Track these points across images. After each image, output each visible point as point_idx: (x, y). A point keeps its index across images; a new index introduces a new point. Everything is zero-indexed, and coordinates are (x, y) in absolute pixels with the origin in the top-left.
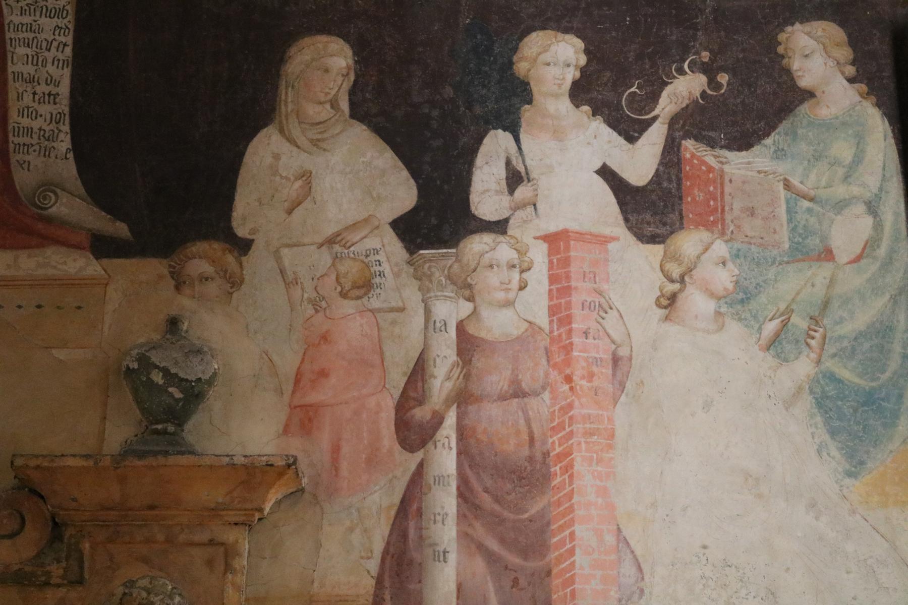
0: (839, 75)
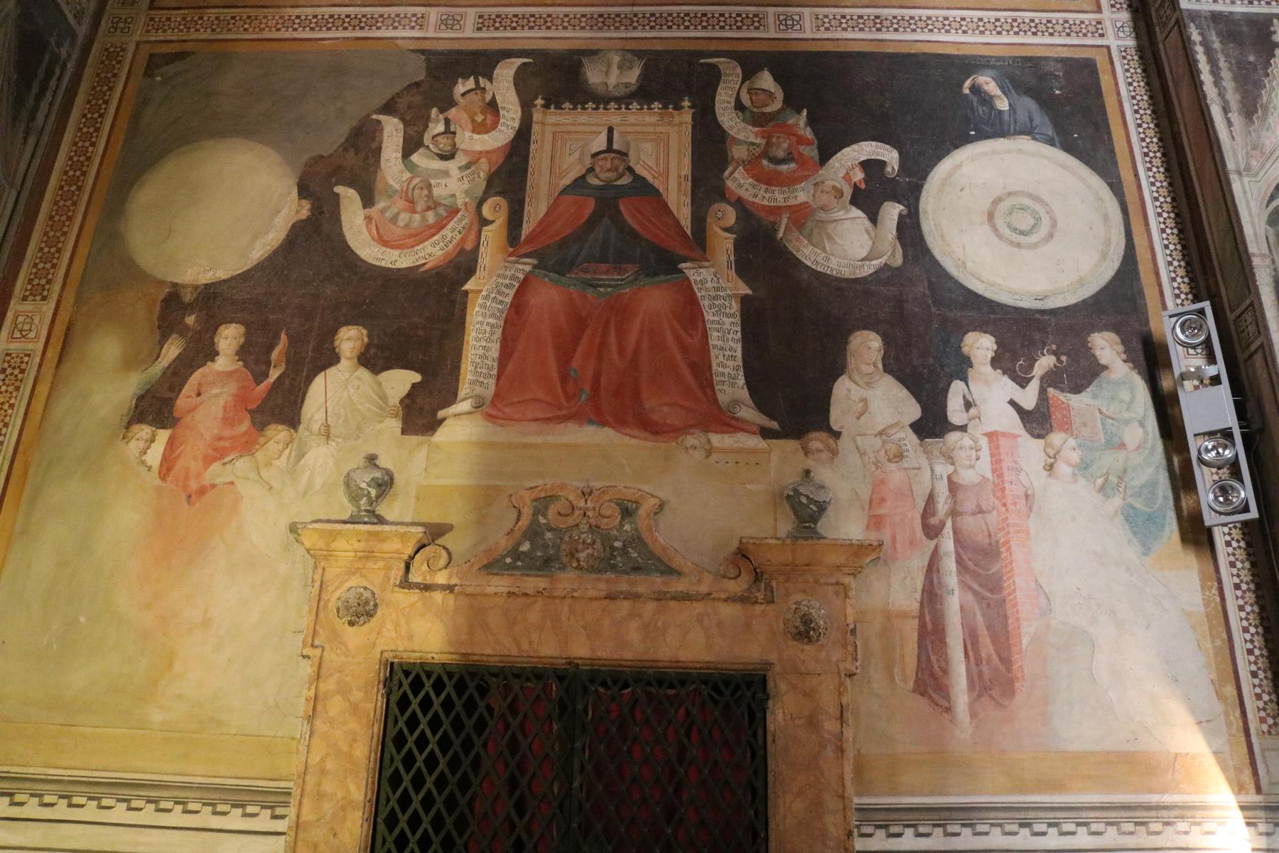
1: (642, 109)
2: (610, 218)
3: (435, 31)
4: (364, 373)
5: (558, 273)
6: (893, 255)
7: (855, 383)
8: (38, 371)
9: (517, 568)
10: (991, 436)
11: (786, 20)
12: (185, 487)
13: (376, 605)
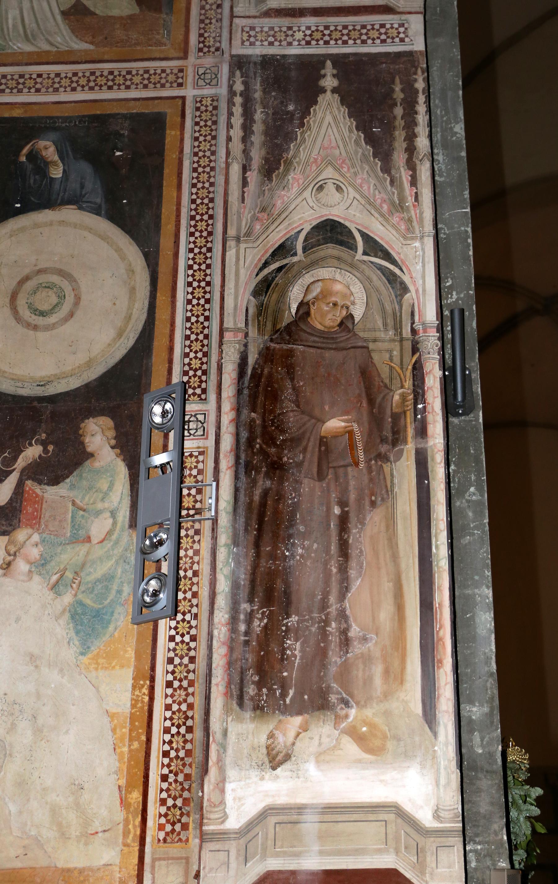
0: (107, 445)
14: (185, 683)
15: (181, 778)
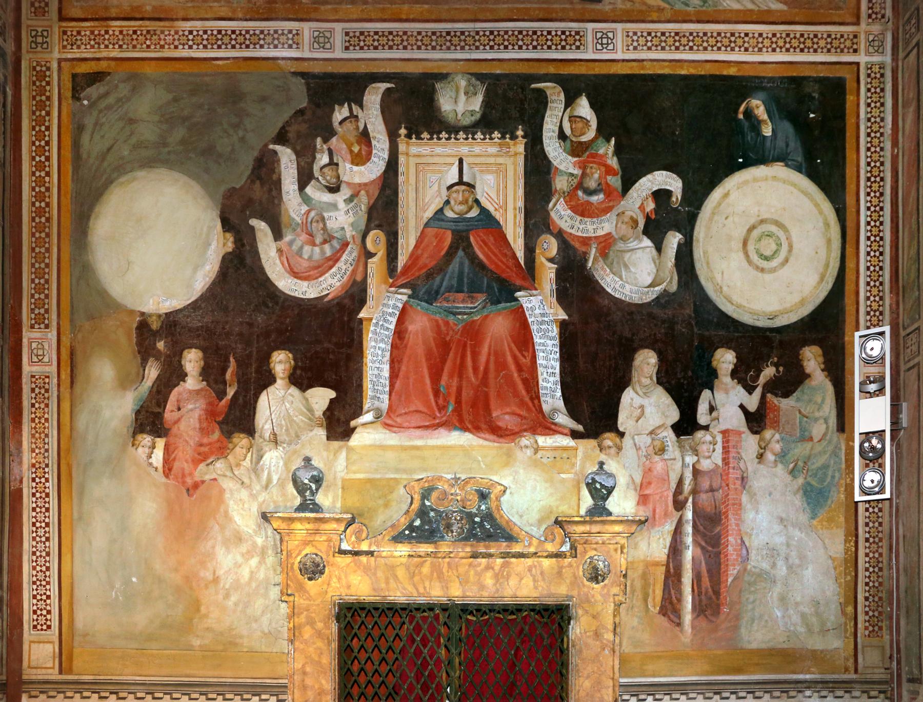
1: (485, 139)
2: (464, 250)
3: (310, 51)
4: (294, 391)
5: (427, 302)
6: (671, 282)
7: (637, 393)
8: (59, 391)
9: (413, 537)
10: (725, 433)
11: (602, 38)
12: (184, 483)
13: (324, 566)
14: (877, 540)
15: (876, 599)
